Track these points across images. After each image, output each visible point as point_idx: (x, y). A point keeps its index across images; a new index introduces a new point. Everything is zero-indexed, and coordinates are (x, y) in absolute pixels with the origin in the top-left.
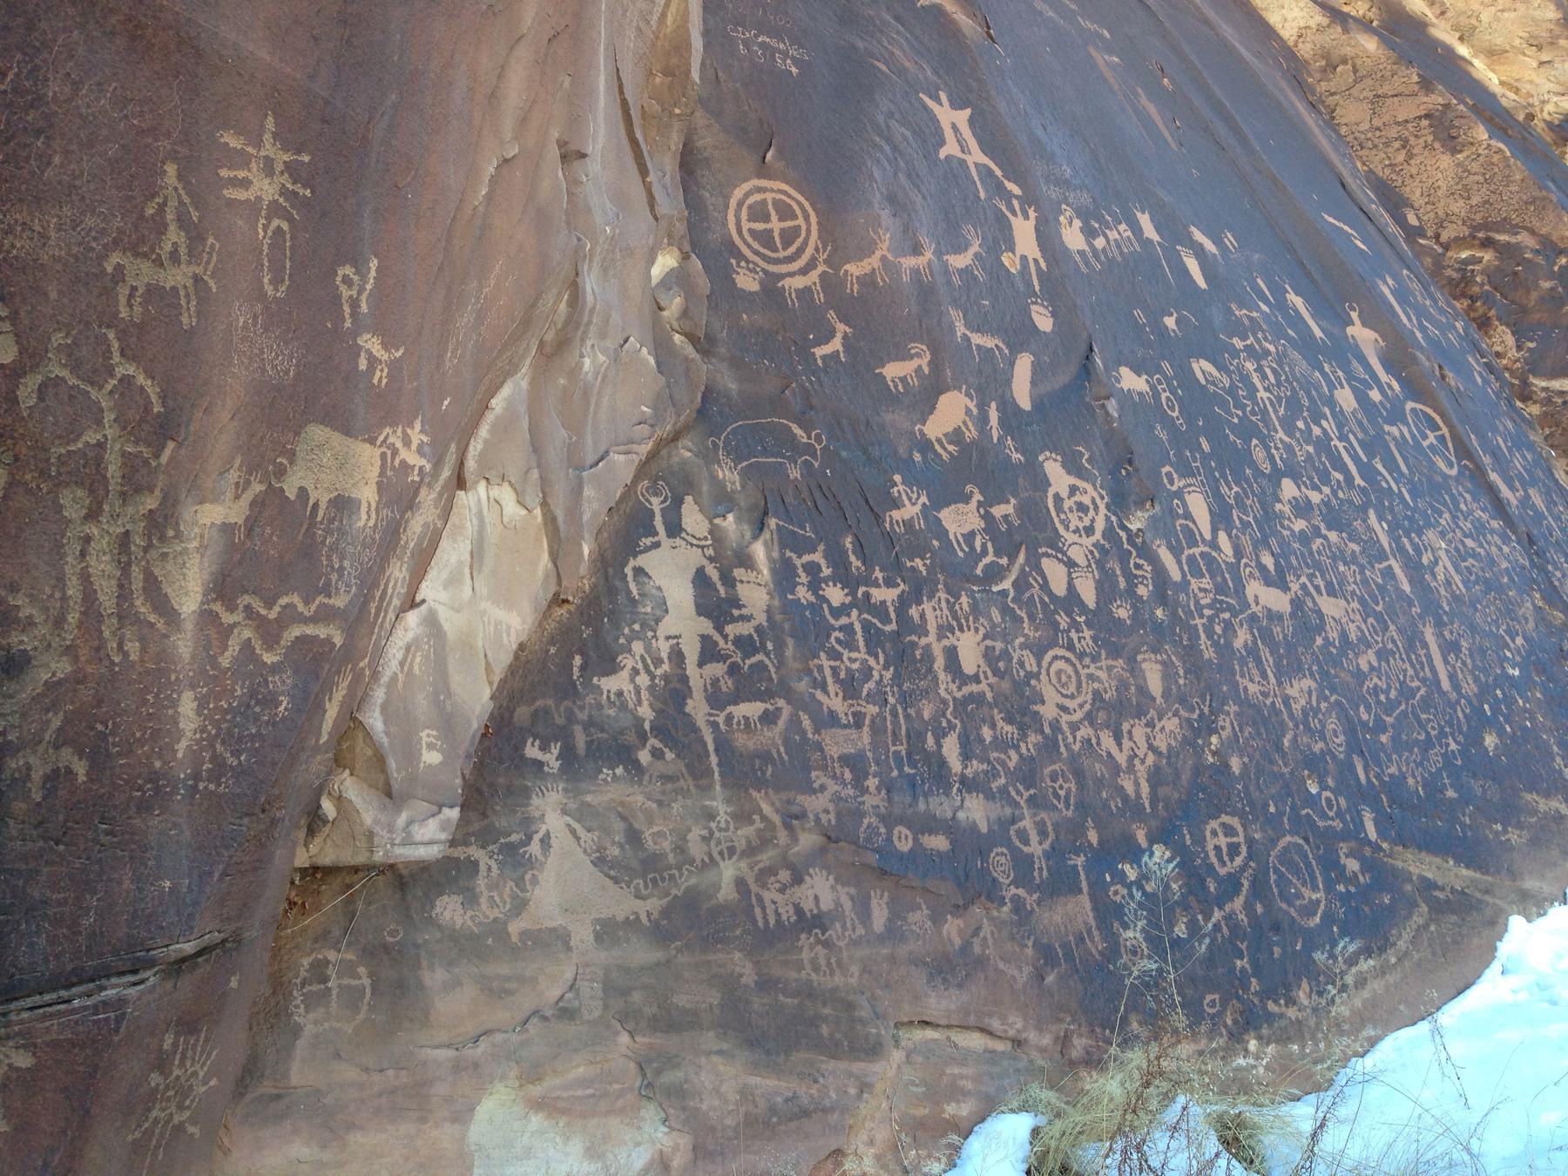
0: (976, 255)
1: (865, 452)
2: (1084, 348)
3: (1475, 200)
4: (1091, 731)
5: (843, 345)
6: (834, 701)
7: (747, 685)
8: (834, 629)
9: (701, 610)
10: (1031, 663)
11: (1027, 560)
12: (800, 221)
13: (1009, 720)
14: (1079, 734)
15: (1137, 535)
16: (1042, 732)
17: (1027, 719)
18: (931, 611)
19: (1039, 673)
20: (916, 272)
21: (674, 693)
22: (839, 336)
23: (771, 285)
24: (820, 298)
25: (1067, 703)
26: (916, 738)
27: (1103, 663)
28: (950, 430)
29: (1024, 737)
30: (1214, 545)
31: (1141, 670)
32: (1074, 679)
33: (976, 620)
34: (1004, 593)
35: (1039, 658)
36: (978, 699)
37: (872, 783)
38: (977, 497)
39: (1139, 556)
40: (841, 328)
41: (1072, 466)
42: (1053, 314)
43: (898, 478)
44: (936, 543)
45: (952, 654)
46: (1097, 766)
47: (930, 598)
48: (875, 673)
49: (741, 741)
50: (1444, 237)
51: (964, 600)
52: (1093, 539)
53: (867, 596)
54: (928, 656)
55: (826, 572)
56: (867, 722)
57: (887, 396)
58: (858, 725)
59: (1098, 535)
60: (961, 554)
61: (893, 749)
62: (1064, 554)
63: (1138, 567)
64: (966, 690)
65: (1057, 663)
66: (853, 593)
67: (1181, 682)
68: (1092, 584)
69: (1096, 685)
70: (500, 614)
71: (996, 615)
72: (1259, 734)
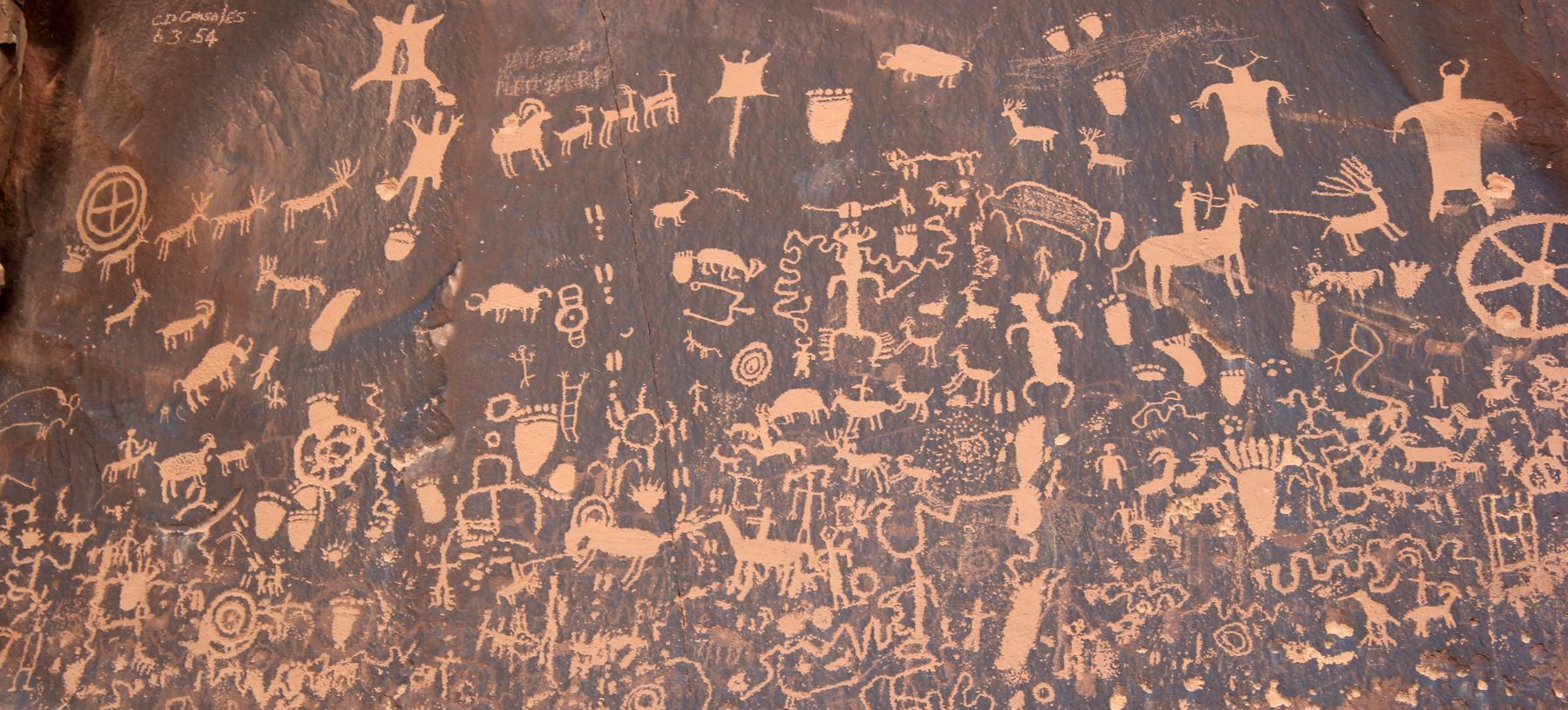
0: (336, 193)
1: (112, 407)
2: (446, 267)
4: (239, 670)
5: (137, 311)
8: (13, 567)
11: (239, 506)
12: (134, 200)
13: (150, 653)
14: (223, 672)
15: (399, 475)
16: (182, 666)
17: (170, 655)
19: (204, 612)
20: (235, 227)
22: (137, 301)
23: (92, 268)
24: (131, 268)
25: (226, 643)
26: (46, 660)
27: (284, 607)
28: (207, 381)
29: (157, 670)
30: (540, 481)
31: (332, 615)
32: (241, 622)
33: (154, 560)
34: (197, 537)
35: (209, 599)
36: (125, 633)
38: (212, 444)
39: (389, 497)
40: (142, 294)
41: (352, 407)
42: (418, 240)
43: (131, 432)
44: (142, 491)
45: (114, 593)
46: (230, 703)
47: (114, 542)
48: (33, 607)
51: (149, 543)
52: (337, 481)
53: (58, 538)
54: (89, 592)
55: (32, 518)
56: (8, 646)
57: (160, 355)
59: (346, 478)
60: (166, 500)
61: (22, 669)
62: (290, 497)
63: (382, 508)
64: (115, 624)
65: (231, 605)
66: (45, 539)
67: (381, 628)
68: (311, 525)
69: (265, 627)
71: (178, 557)
72: (482, 690)
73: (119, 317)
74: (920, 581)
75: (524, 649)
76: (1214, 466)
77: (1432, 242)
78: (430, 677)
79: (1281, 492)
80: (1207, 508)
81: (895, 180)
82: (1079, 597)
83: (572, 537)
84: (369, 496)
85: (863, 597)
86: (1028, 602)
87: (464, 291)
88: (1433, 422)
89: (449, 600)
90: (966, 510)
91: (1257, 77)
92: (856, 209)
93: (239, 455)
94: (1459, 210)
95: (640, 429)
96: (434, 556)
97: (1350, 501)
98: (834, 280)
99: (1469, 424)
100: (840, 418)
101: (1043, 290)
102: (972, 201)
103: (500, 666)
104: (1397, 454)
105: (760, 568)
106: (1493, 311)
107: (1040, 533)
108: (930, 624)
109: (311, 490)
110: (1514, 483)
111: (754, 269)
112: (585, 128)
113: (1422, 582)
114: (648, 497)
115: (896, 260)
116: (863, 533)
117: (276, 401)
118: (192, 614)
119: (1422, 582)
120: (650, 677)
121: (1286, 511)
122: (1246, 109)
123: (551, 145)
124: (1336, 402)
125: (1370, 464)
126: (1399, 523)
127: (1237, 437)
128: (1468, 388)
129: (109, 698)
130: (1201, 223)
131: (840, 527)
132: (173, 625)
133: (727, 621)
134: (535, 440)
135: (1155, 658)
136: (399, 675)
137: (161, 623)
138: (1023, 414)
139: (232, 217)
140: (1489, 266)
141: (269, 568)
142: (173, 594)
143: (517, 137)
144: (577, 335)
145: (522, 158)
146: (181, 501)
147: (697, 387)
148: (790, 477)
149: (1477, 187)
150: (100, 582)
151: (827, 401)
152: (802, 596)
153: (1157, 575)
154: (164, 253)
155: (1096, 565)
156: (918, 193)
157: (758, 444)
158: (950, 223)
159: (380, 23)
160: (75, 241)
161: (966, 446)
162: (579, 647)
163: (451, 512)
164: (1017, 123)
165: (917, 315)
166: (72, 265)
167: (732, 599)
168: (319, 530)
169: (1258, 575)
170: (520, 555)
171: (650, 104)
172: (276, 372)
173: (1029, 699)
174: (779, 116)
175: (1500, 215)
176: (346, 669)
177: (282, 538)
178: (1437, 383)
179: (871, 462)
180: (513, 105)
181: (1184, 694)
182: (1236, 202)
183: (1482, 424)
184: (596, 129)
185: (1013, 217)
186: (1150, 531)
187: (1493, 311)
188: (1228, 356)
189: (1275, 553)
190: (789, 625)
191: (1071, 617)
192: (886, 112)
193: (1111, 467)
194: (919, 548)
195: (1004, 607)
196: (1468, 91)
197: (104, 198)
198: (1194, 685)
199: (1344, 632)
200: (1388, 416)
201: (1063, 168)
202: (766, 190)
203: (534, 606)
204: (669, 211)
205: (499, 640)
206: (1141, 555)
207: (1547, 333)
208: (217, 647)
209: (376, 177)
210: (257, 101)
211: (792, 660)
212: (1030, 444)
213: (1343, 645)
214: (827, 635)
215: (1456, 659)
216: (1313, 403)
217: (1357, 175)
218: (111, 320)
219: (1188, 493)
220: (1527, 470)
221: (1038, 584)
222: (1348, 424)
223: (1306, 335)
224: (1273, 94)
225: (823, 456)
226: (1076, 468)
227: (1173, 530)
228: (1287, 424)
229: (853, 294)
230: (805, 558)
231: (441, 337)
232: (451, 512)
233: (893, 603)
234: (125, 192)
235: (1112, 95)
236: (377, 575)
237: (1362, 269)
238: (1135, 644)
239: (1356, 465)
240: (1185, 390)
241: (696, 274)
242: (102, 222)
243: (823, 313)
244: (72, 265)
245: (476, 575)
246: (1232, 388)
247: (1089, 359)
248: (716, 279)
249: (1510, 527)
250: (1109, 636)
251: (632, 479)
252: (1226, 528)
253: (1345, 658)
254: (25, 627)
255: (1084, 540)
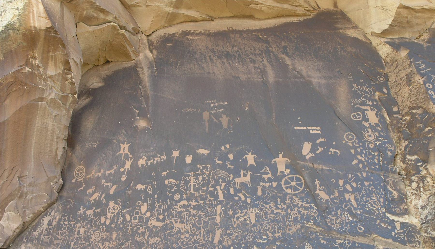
3: (411, 101)
6: (59, 237)
7: (48, 234)
9: (48, 225)
10: (92, 233)
18: (78, 225)
21: (40, 234)
23: (76, 181)
24: (82, 181)
25: (96, 239)
26: (68, 242)
29: (85, 243)
30: (145, 214)
37: (59, 247)
41: (116, 203)
49: (45, 240)
50: (403, 113)
51: (84, 223)
57: (87, 195)
58: (61, 240)
59: (115, 214)
65: (97, 233)
70: (14, 225)
71: (89, 226)
72: (135, 246)
73: (80, 189)
74: (202, 230)
75: (142, 240)
76: (246, 212)
77: (278, 179)
78: (127, 244)
79: (256, 216)
80: (245, 219)
81: (198, 169)
82: (226, 232)
83: (149, 223)
84: (118, 216)
85: (194, 232)
86: (218, 233)
87: (133, 186)
88: (278, 206)
89: (130, 232)
90: (209, 219)
91: (252, 154)
92: (193, 173)
93: (99, 210)
94: (282, 174)
95: (160, 207)
96: (128, 226)
97: (266, 218)
98: (189, 184)
99: (283, 206)
100: (190, 205)
101: (221, 186)
102: (210, 172)
103: (138, 243)
104: (273, 211)
105: (178, 228)
106: (287, 189)
107: (220, 223)
108: (204, 236)
109: (110, 215)
110: (290, 215)
111: (177, 182)
112: (152, 161)
113: (277, 230)
114: (161, 217)
115: (199, 181)
116: (194, 222)
117: (104, 202)
118: (91, 234)
119: (277, 230)
120: (161, 244)
121: (257, 219)
122: (251, 159)
123: (147, 163)
124: (264, 203)
125: (269, 212)
126: (273, 221)
127: (249, 208)
128: (283, 201)
129: (78, 247)
130: (244, 176)
131: (190, 222)
132: (88, 236)
133: (173, 236)
134: (144, 208)
135: (237, 241)
136: (123, 244)
137: (86, 236)
138: (218, 204)
139: (98, 174)
140: (286, 183)
141: (103, 228)
142: (88, 232)
143: (142, 162)
144: (150, 192)
145: (142, 165)
146: (89, 217)
147: (168, 200)
148: (182, 214)
149: (284, 171)
150: (77, 230)
151: (188, 202)
152: (184, 232)
153: (238, 229)
154: (88, 179)
155: (228, 227)
156: (202, 171)
157: (178, 209)
158: (207, 176)
159: (121, 144)
160: (74, 177)
161: (209, 209)
162: (150, 240)
163: (131, 219)
164: (217, 161)
165: (202, 189)
166: (73, 181)
167: (174, 233)
168: (111, 222)
169: (253, 229)
170: (141, 226)
171: (162, 157)
172: (104, 197)
173: (218, 247)
174: (181, 159)
175: (288, 175)
176: (115, 243)
177: (105, 223)
178: (279, 200)
179: (195, 212)
180: (141, 157)
181: (242, 247)
182: (249, 173)
183: (285, 206)
184: (154, 161)
185: (216, 175)
186: (237, 222)
187: (287, 189)
188: (248, 196)
189: (254, 225)
190: (182, 236)
191: (225, 235)
192: (197, 159)
193: (231, 213)
194: (202, 225)
195: (215, 234)
196: (283, 157)
197: (78, 171)
198: (243, 245)
199: (265, 237)
200: (272, 205)
201: (223, 167)
202: (179, 170)
203: (143, 233)
204: (164, 173)
205: (138, 239)
206: (235, 226)
207: (295, 193)
208: (95, 240)
209: (120, 168)
210: (102, 156)
211: (183, 242)
212: (219, 209)
213: (265, 239)
214: (188, 238)
215: (282, 242)
216: (261, 203)
217: (267, 169)
218: (79, 189)
219: (242, 216)
220: (292, 213)
221: (220, 230)
222: (266, 206)
223: (259, 193)
224: (254, 157)
225: (188, 211)
226: (225, 213)
227: (240, 222)
228: (257, 206)
229: (192, 186)
230: (185, 226)
231: (130, 192)
232: (131, 219)
233: (198, 233)
234: (82, 170)
235: (231, 157)
236: (120, 229)
237: (268, 183)
238: (234, 239)
239: (267, 212)
240: (242, 201)
241: (169, 183)
242: (78, 174)
243: (188, 189)
244: (73, 181)
245: (135, 229)
246: (249, 201)
247: (227, 196)
248: (172, 184)
249: (289, 221)
250: (230, 238)
251: (159, 214)
252: (248, 222)
253: (266, 241)
254: (65, 236)
255: (227, 223)
